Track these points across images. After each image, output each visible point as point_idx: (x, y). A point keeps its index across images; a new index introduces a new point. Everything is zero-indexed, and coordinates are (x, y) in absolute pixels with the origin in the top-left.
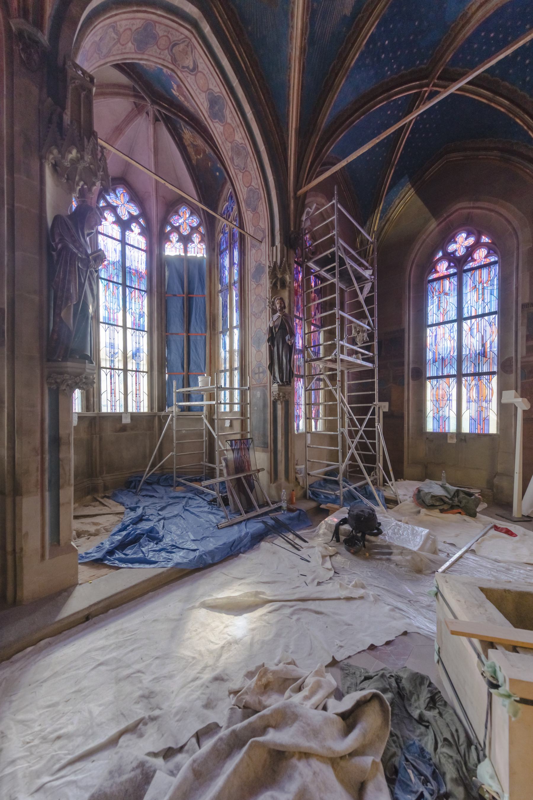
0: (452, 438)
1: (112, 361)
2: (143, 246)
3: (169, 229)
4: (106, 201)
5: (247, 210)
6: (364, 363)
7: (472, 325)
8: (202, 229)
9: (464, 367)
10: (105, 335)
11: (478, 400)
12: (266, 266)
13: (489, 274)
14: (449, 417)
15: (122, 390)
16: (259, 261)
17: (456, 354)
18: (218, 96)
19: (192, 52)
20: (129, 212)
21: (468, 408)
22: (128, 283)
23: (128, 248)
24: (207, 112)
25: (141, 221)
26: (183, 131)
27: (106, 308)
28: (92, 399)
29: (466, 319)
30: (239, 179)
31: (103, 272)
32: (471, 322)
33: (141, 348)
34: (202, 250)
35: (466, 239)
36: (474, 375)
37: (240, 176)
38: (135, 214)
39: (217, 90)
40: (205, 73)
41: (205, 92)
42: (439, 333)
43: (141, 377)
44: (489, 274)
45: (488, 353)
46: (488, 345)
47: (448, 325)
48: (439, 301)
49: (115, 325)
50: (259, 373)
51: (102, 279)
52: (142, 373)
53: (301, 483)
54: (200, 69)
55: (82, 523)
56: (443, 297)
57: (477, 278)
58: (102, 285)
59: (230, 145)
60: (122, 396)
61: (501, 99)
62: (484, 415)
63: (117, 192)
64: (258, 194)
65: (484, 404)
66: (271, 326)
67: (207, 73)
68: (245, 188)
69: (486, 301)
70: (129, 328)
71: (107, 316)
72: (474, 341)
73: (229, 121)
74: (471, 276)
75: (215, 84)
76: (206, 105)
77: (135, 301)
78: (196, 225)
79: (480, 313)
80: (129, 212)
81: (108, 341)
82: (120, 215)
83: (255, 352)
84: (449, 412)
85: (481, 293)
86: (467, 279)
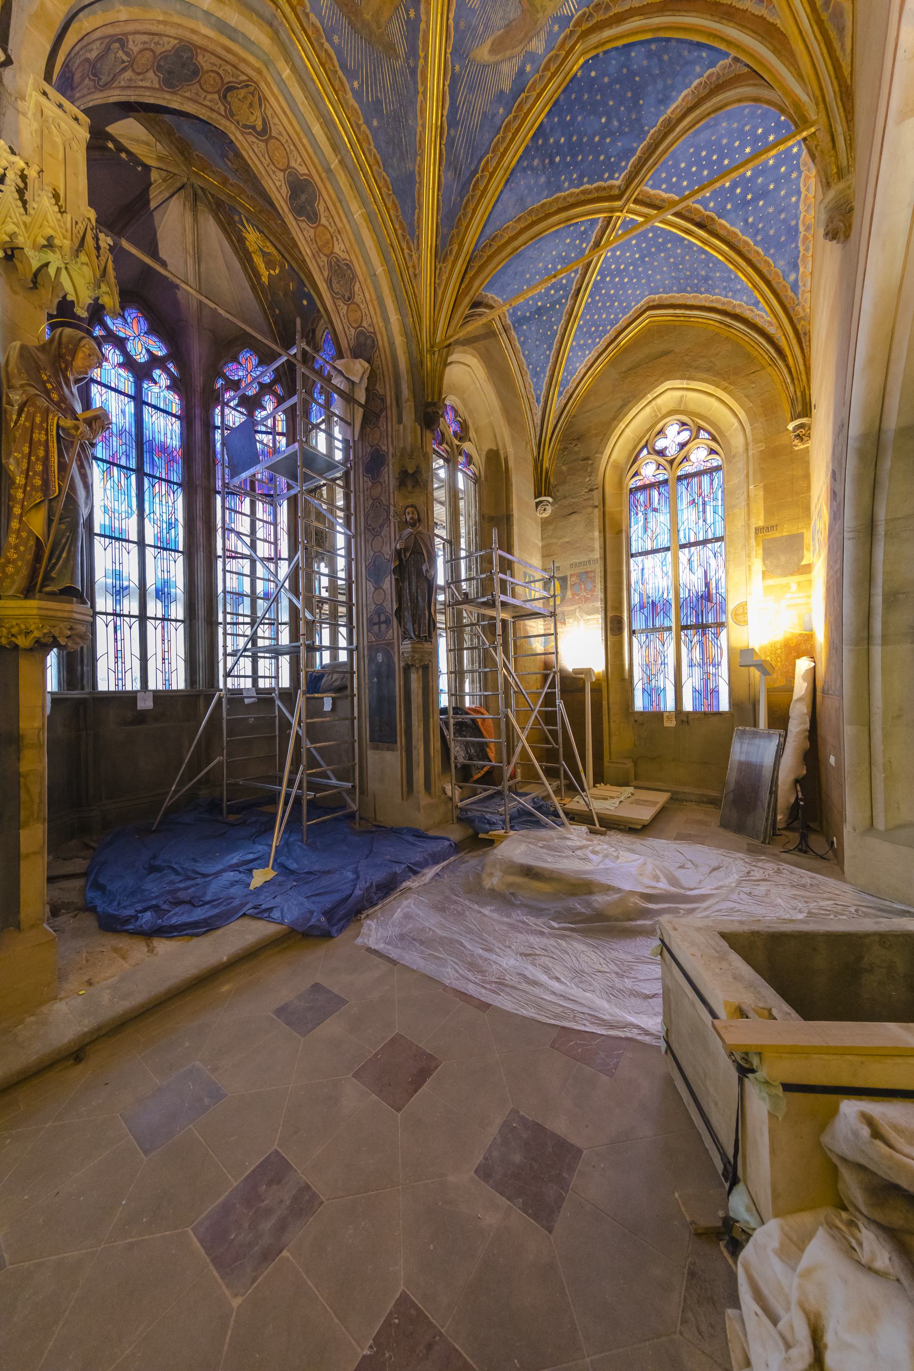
2: (175, 409)
3: (220, 383)
4: (105, 327)
10: (103, 557)
11: (703, 664)
12: (388, 453)
13: (711, 484)
16: (377, 445)
18: (305, 180)
19: (260, 105)
20: (148, 351)
21: (690, 676)
22: (147, 469)
23: (146, 410)
24: (286, 203)
25: (171, 366)
27: (106, 510)
28: (79, 668)
32: (689, 551)
33: (173, 579)
37: (343, 308)
38: (160, 354)
39: (303, 170)
40: (283, 141)
41: (283, 171)
43: (173, 630)
44: (711, 484)
45: (714, 596)
46: (714, 585)
47: (659, 556)
48: (646, 519)
49: (123, 540)
50: (379, 623)
52: (174, 623)
54: (274, 134)
55: (60, 889)
56: (651, 515)
57: (696, 489)
58: (97, 472)
59: (325, 259)
60: (137, 664)
61: (714, 240)
62: (711, 685)
63: (126, 314)
64: (373, 341)
65: (712, 670)
66: (398, 547)
67: (287, 141)
68: (351, 329)
69: (708, 522)
71: (107, 523)
72: (694, 578)
73: (323, 221)
74: (688, 484)
75: (299, 160)
76: (285, 190)
77: (161, 501)
78: (269, 381)
79: (701, 539)
80: (148, 351)
81: (109, 567)
82: (133, 353)
83: (373, 588)
84: (664, 682)
85: (701, 509)
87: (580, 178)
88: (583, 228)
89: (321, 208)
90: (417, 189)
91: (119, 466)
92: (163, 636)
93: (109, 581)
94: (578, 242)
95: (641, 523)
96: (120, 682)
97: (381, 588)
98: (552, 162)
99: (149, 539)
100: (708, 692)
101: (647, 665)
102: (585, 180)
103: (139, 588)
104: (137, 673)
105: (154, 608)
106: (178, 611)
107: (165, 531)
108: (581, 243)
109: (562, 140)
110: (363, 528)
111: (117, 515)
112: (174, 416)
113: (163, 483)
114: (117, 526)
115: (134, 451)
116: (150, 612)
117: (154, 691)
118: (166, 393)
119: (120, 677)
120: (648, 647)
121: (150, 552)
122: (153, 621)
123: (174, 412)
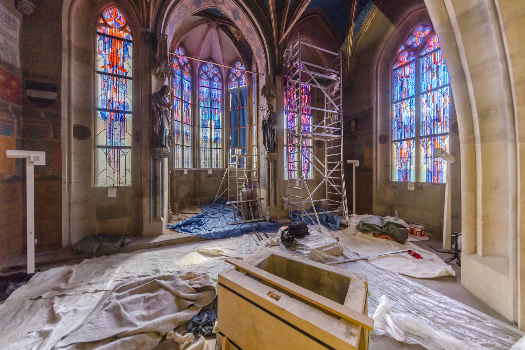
0: (411, 186)
1: (205, 145)
6: (333, 136)
7: (428, 98)
9: (421, 131)
14: (410, 170)
17: (414, 122)
21: (425, 163)
27: (203, 120)
29: (423, 93)
35: (423, 31)
36: (430, 136)
42: (402, 107)
47: (409, 100)
53: (286, 208)
62: (438, 168)
72: (429, 109)
84: (410, 166)
86: (424, 62)
95: (400, 85)
99: (213, 126)
100: (434, 172)
101: (401, 158)
105: (214, 146)
106: (220, 146)
116: (213, 147)
120: (401, 149)
121: (213, 130)
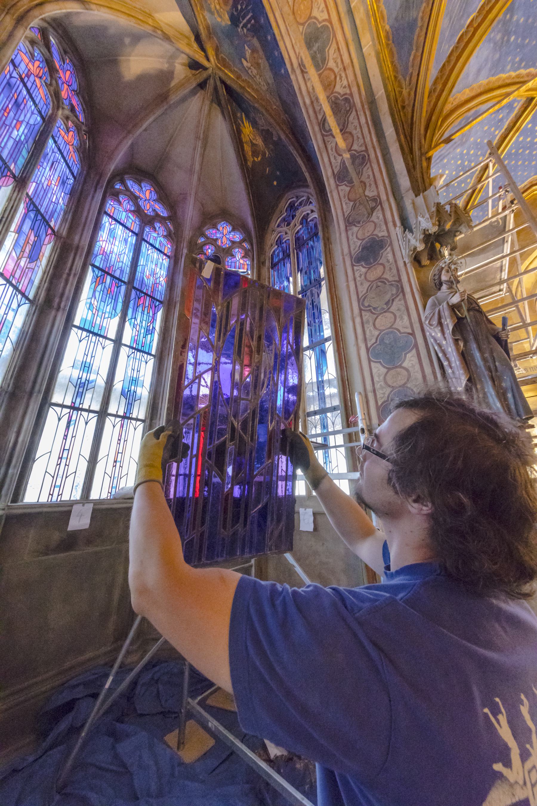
5: (337, 186)
8: (246, 245)
15: (87, 455)
23: (144, 244)
26: (243, 123)
30: (329, 149)
31: (99, 258)
33: (141, 379)
34: (246, 267)
49: (100, 336)
51: (94, 266)
60: (83, 466)
63: (143, 185)
70: (126, 345)
71: (89, 318)
77: (143, 311)
81: (80, 358)
87: (521, 61)
88: (501, 116)
89: (332, 51)
90: (417, 33)
91: (112, 276)
92: (120, 435)
93: (76, 373)
94: (493, 129)
96: (57, 490)
97: (400, 366)
98: (508, 40)
102: (523, 64)
103: (106, 383)
104: (81, 479)
107: (142, 335)
108: (495, 130)
109: (522, 20)
110: (356, 311)
111: (100, 314)
112: (165, 255)
113: (148, 298)
114: (98, 322)
115: (128, 269)
117: (96, 502)
118: (162, 239)
119: (58, 483)
121: (124, 351)
122: (112, 418)
123: (166, 252)
